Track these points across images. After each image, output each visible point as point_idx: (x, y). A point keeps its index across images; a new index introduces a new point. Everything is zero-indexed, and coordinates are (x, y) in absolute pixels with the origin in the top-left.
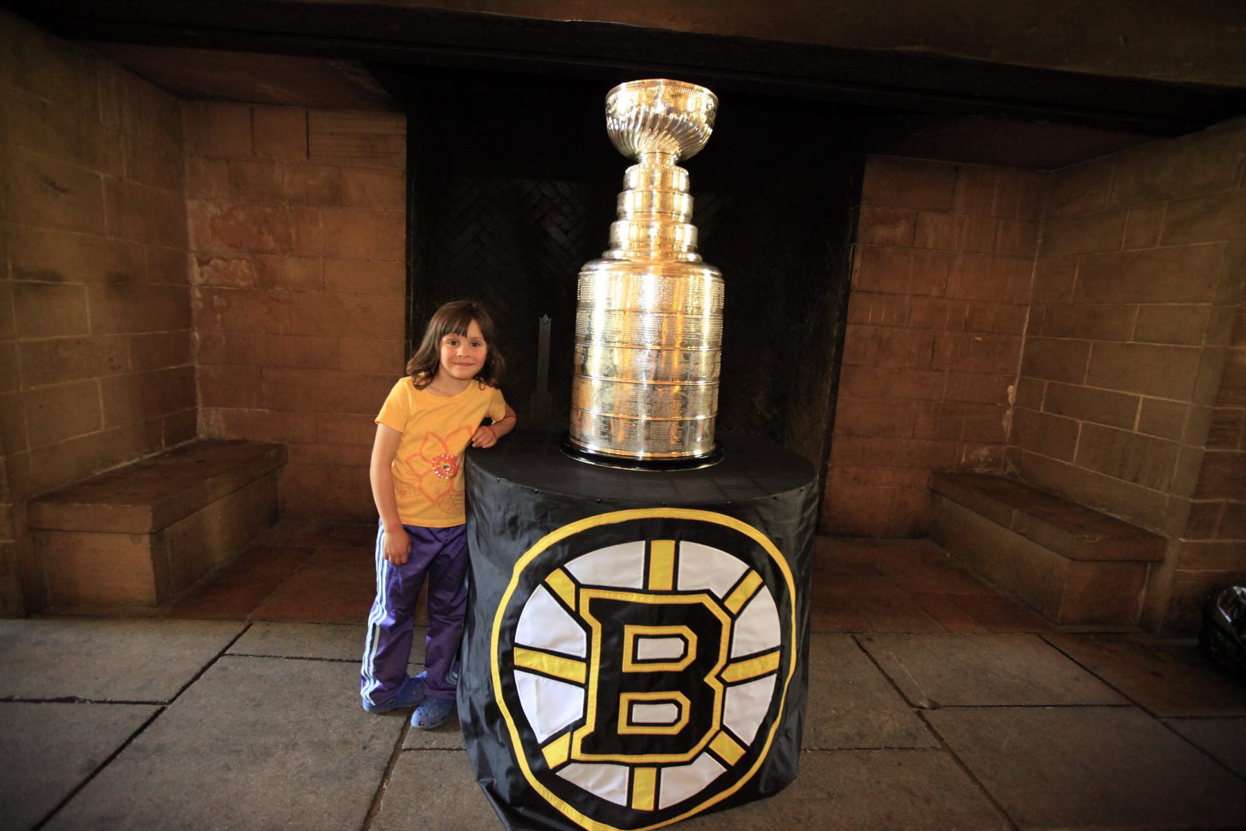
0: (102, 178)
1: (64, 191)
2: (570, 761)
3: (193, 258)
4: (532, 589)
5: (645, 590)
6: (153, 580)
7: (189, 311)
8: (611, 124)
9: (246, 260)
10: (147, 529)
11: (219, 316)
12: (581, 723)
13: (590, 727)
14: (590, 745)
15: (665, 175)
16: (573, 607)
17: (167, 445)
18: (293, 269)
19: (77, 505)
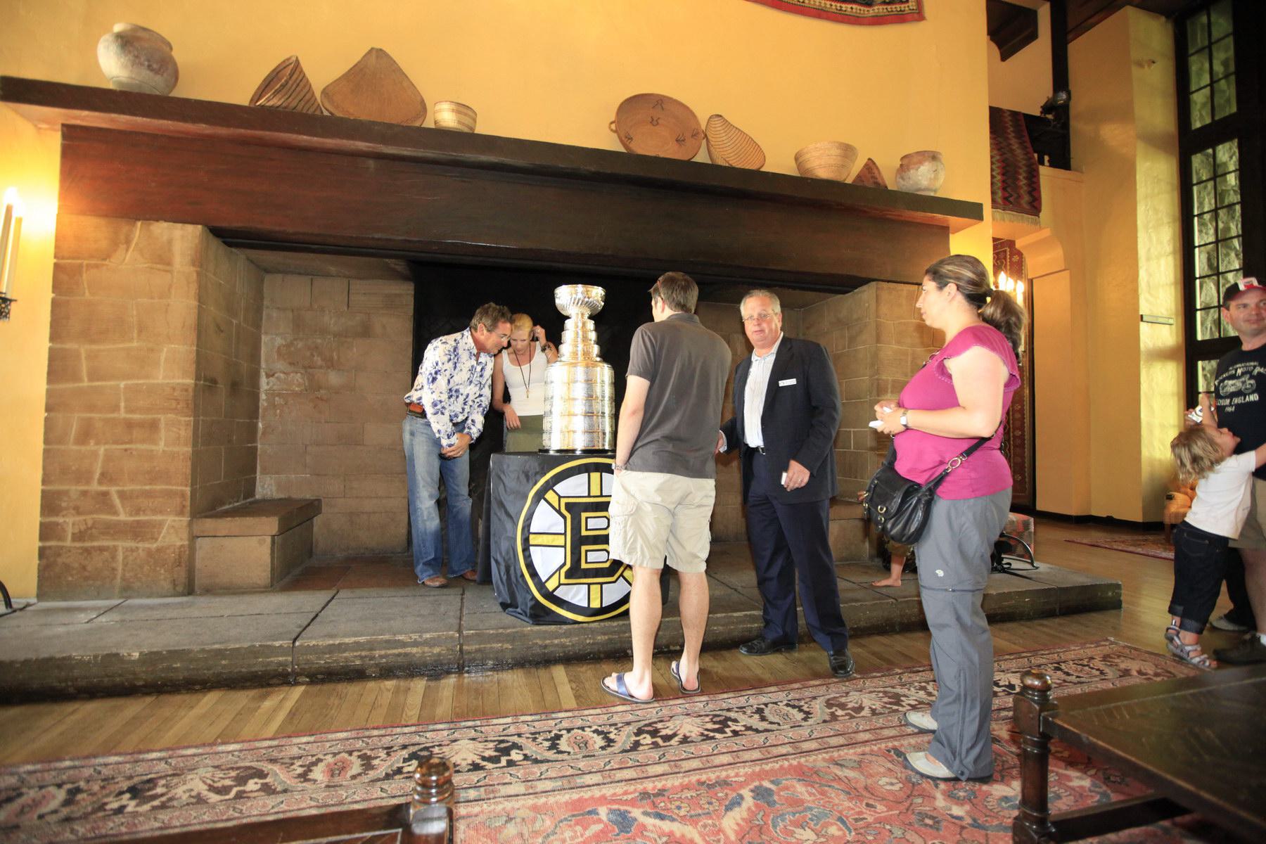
0: (234, 322)
1: (222, 331)
2: (560, 585)
3: (263, 374)
4: (539, 501)
5: (589, 496)
6: (269, 569)
7: (258, 408)
8: (558, 301)
9: (302, 374)
10: (274, 533)
11: (278, 411)
12: (564, 564)
13: (568, 565)
14: (569, 575)
15: (584, 324)
16: (557, 508)
17: (245, 498)
18: (334, 378)
19: (229, 519)
